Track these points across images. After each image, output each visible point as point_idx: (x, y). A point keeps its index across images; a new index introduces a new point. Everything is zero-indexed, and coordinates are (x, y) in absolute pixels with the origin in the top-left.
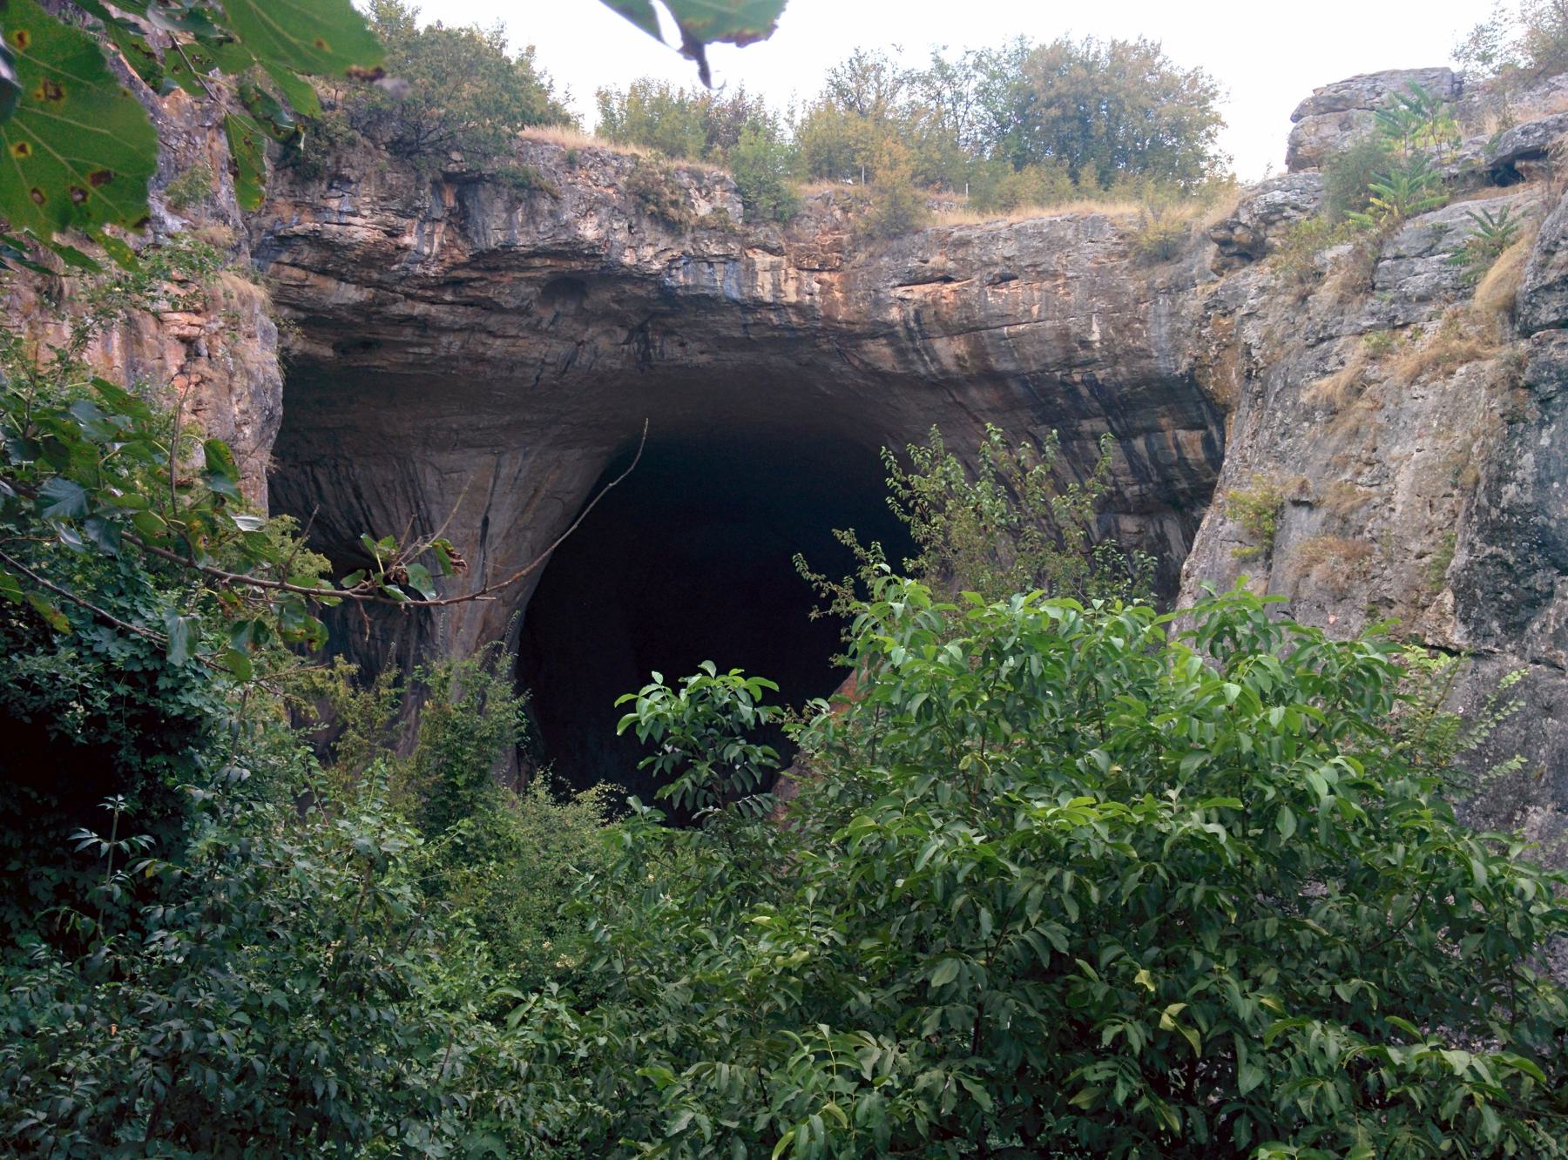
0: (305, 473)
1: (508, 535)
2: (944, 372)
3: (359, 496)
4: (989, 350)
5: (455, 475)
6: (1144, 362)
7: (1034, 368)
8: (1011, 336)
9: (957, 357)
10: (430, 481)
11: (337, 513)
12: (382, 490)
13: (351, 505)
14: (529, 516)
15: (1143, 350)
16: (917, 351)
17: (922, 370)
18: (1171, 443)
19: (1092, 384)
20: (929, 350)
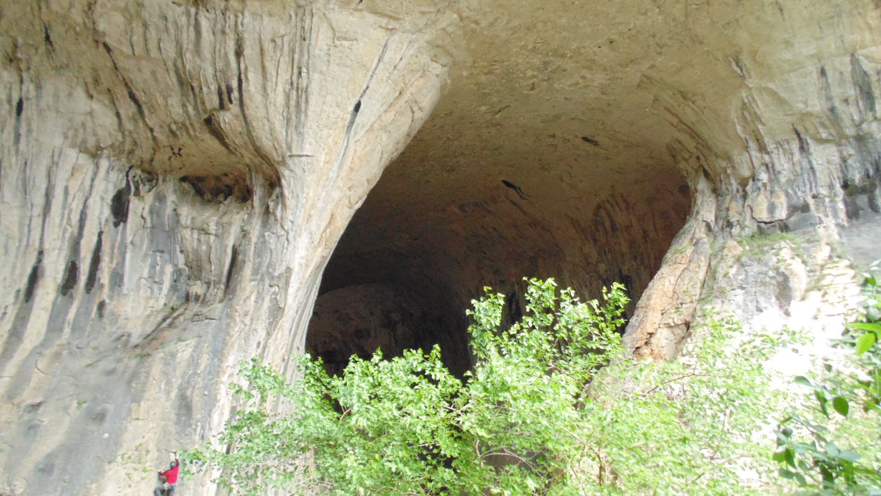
0: (188, 14)
1: (371, 129)
3: (239, 54)
5: (346, 43)
10: (321, 40)
11: (210, 71)
12: (268, 46)
13: (227, 64)
14: (390, 116)
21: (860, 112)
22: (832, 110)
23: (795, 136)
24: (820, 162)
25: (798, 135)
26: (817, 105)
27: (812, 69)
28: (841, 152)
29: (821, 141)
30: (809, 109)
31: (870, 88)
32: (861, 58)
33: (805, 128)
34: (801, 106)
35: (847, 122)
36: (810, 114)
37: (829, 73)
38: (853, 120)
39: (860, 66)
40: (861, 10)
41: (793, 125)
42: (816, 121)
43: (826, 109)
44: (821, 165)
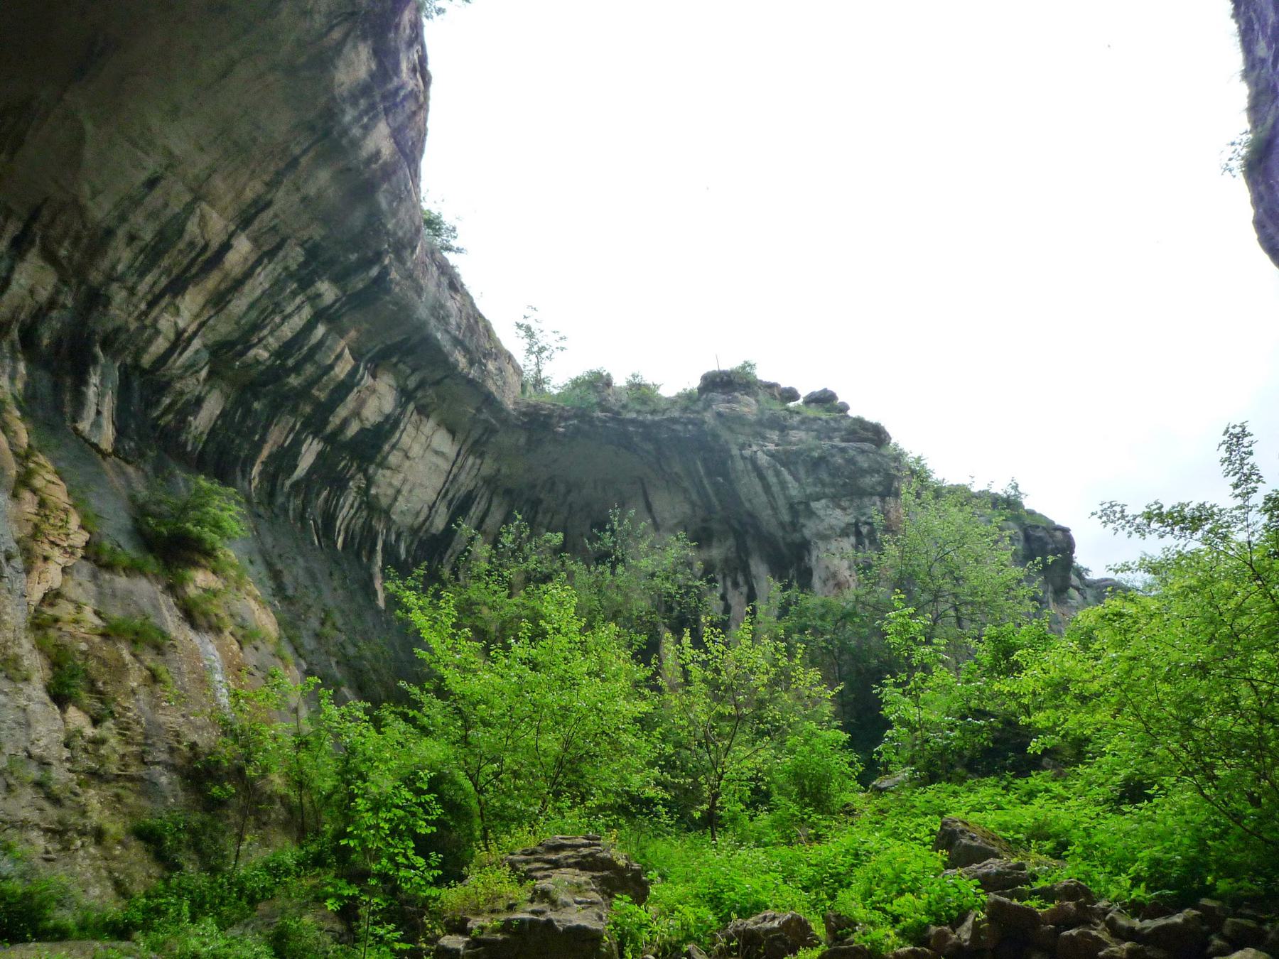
2: (356, 144)
4: (394, 179)
6: (416, 298)
7: (389, 226)
8: (409, 191)
9: (377, 154)
15: (422, 289)
16: (372, 107)
17: (348, 118)
18: (339, 350)
19: (385, 272)
20: (374, 119)
21: (129, 268)
22: (110, 233)
23: (26, 216)
24: (22, 281)
25: (34, 215)
26: (100, 211)
27: (152, 164)
28: (57, 292)
29: (50, 256)
30: (90, 204)
31: (166, 252)
32: (198, 211)
33: (53, 221)
34: (87, 189)
35: (105, 264)
36: (81, 211)
37: (158, 191)
38: (113, 268)
39: (187, 219)
40: (258, 169)
41: (46, 200)
42: (76, 225)
43: (104, 225)
44: (21, 286)
